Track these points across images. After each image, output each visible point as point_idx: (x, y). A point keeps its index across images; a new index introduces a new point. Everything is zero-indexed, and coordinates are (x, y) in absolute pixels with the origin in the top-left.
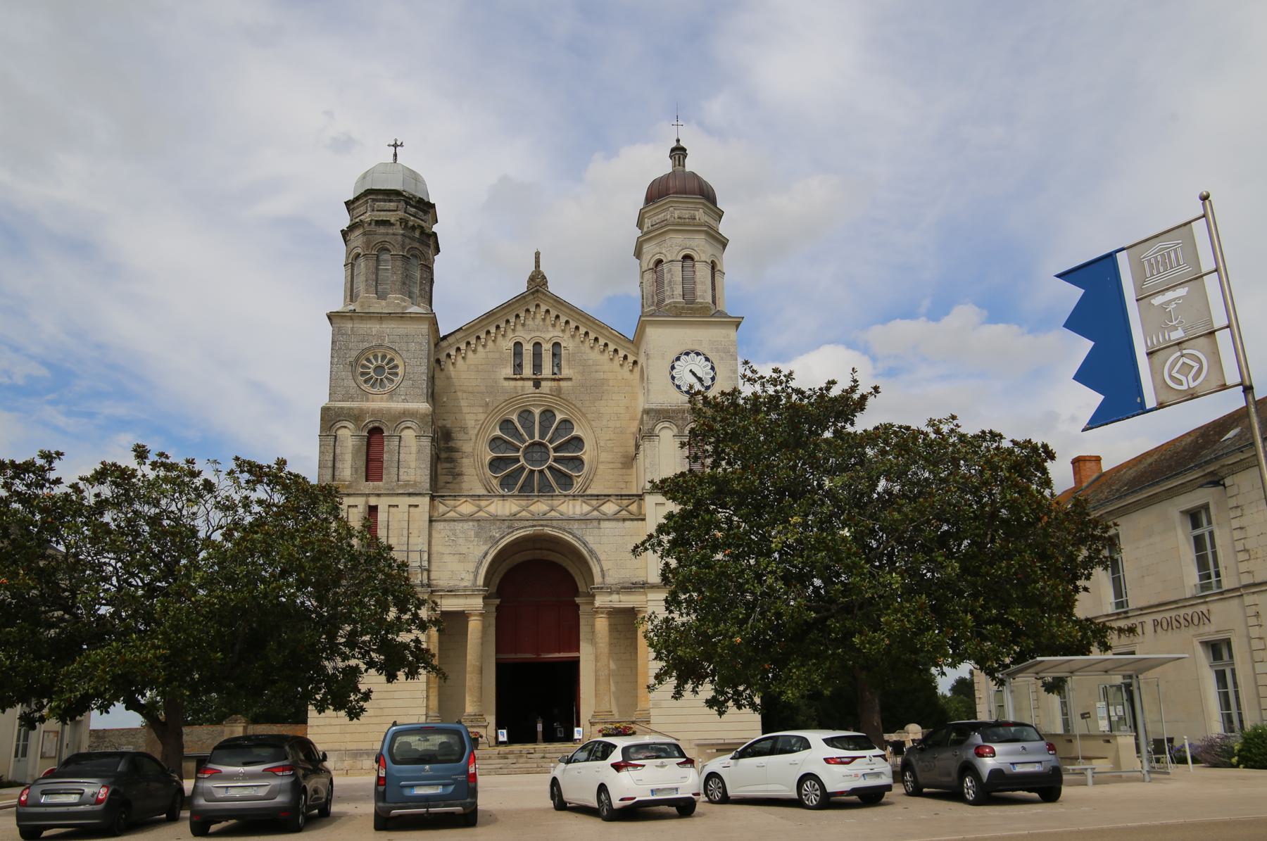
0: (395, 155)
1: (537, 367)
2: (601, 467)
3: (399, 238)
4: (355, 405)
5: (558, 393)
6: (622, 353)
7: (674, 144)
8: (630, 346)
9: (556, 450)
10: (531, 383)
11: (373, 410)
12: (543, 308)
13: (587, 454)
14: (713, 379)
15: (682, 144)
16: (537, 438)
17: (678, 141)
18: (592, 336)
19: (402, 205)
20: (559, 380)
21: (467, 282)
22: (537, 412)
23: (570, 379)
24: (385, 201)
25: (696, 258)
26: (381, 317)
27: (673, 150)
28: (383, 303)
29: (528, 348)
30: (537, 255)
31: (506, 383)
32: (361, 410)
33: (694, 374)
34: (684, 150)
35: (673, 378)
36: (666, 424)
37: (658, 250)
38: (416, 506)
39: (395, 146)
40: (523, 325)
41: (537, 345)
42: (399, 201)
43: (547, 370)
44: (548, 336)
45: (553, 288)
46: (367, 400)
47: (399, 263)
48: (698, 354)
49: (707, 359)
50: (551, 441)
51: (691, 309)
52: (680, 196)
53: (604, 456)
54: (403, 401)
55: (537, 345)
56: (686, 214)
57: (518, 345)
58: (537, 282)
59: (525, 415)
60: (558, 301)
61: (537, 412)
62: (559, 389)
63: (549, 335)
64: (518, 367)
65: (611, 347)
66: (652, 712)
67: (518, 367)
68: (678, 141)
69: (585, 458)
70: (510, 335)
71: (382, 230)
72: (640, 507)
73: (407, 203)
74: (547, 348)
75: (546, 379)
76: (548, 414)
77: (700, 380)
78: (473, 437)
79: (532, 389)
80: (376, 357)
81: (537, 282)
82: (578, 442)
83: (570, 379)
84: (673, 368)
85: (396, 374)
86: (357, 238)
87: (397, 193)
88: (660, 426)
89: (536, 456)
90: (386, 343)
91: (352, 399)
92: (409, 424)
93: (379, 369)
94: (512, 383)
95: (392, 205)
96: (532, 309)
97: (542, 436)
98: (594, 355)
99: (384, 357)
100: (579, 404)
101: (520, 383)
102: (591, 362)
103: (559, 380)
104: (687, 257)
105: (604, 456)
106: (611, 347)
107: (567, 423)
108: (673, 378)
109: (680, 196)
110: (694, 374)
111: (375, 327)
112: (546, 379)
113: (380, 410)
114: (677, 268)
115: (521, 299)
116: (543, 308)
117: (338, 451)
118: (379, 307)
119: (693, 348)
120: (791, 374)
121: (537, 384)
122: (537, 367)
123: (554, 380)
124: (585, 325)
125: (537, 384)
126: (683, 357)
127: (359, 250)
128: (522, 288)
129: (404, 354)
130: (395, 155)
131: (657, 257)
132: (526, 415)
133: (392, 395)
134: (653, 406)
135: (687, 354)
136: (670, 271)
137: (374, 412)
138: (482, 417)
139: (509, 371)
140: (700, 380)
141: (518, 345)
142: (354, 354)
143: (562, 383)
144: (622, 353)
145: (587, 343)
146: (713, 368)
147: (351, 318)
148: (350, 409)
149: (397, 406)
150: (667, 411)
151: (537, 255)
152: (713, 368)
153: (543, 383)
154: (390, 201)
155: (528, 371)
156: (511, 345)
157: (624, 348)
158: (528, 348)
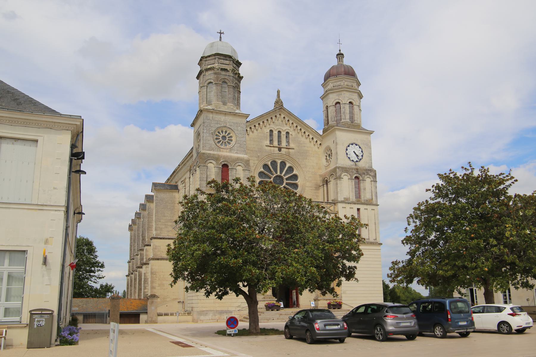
0: (221, 37)
1: (279, 142)
2: (307, 188)
3: (231, 78)
4: (215, 153)
5: (288, 155)
6: (315, 140)
7: (338, 52)
8: (320, 137)
9: (287, 179)
10: (277, 149)
11: (224, 156)
12: (283, 116)
13: (299, 182)
14: (362, 156)
15: (342, 52)
16: (279, 173)
17: (340, 50)
18: (303, 131)
19: (231, 62)
20: (289, 149)
21: (254, 100)
22: (279, 162)
23: (293, 149)
24: (224, 59)
25: (354, 103)
26: (225, 113)
27: (338, 55)
28: (226, 107)
29: (275, 133)
30: (278, 92)
31: (267, 148)
32: (219, 155)
33: (355, 153)
34: (342, 54)
35: (347, 154)
36: (346, 174)
37: (337, 97)
38: (345, 216)
39: (221, 33)
40: (273, 122)
41: (279, 132)
42: (230, 61)
43: (284, 144)
44: (284, 129)
45: (285, 106)
46: (220, 151)
47: (231, 89)
48: (356, 145)
49: (360, 148)
50: (284, 175)
51: (353, 125)
52: (341, 74)
53: (308, 184)
54: (236, 153)
55: (279, 132)
56: (350, 84)
57: (271, 131)
58: (279, 105)
59: (283, 164)
60: (290, 113)
61: (279, 162)
62: (289, 153)
63: (285, 128)
64: (271, 141)
65: (311, 137)
66: (343, 295)
67: (271, 141)
68: (340, 50)
69: (299, 184)
70: (268, 126)
71: (223, 73)
72: (334, 208)
73: (233, 62)
74: (283, 134)
75: (284, 148)
76: (283, 164)
77: (357, 156)
78: (253, 171)
79: (278, 152)
80: (222, 132)
81: (279, 105)
82: (295, 177)
83: (293, 149)
84: (347, 150)
85: (231, 140)
86: (209, 76)
87: (230, 57)
88: (344, 174)
89: (278, 181)
90: (228, 126)
91: (213, 149)
92: (240, 164)
93: (224, 137)
94: (269, 148)
95: (227, 62)
96: (278, 116)
97: (281, 172)
98: (303, 139)
99: (226, 132)
100: (297, 160)
101: (272, 148)
102: (302, 142)
103: (289, 149)
104: (350, 103)
105: (308, 184)
106: (311, 137)
107: (291, 169)
108: (347, 154)
109: (341, 74)
110: (355, 153)
111: (222, 118)
112: (284, 148)
113: (227, 156)
114: (347, 107)
115: (274, 111)
116: (283, 116)
117: (208, 173)
118: (224, 108)
119: (354, 142)
120: (488, 169)
121: (280, 149)
122: (279, 142)
123: (287, 148)
124: (300, 125)
125: (280, 149)
126: (351, 145)
127: (212, 81)
128: (271, 107)
129: (236, 132)
130: (221, 37)
131: (337, 101)
132: (274, 163)
133: (231, 149)
134: (340, 165)
135: (352, 144)
136: (344, 108)
137: (224, 157)
138: (257, 162)
139: (268, 143)
140: (357, 156)
141: (271, 131)
142: (214, 129)
143: (290, 150)
144: (315, 140)
145: (300, 134)
146: (362, 151)
147: (212, 112)
148: (214, 154)
149: (234, 155)
150: (346, 168)
151: (278, 92)
152: (362, 151)
153: (282, 149)
154: (226, 60)
155: (276, 143)
156: (268, 131)
157: (316, 137)
158: (275, 133)
